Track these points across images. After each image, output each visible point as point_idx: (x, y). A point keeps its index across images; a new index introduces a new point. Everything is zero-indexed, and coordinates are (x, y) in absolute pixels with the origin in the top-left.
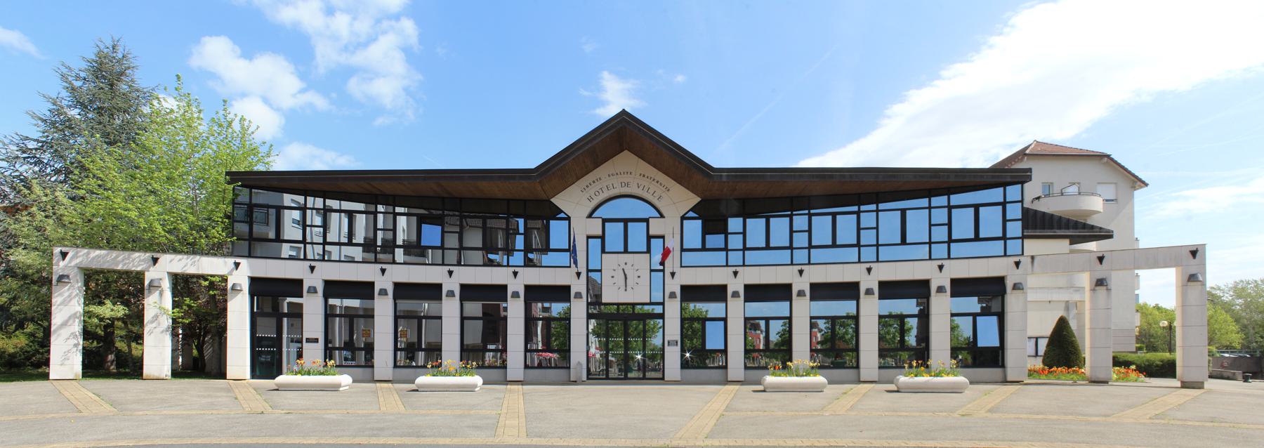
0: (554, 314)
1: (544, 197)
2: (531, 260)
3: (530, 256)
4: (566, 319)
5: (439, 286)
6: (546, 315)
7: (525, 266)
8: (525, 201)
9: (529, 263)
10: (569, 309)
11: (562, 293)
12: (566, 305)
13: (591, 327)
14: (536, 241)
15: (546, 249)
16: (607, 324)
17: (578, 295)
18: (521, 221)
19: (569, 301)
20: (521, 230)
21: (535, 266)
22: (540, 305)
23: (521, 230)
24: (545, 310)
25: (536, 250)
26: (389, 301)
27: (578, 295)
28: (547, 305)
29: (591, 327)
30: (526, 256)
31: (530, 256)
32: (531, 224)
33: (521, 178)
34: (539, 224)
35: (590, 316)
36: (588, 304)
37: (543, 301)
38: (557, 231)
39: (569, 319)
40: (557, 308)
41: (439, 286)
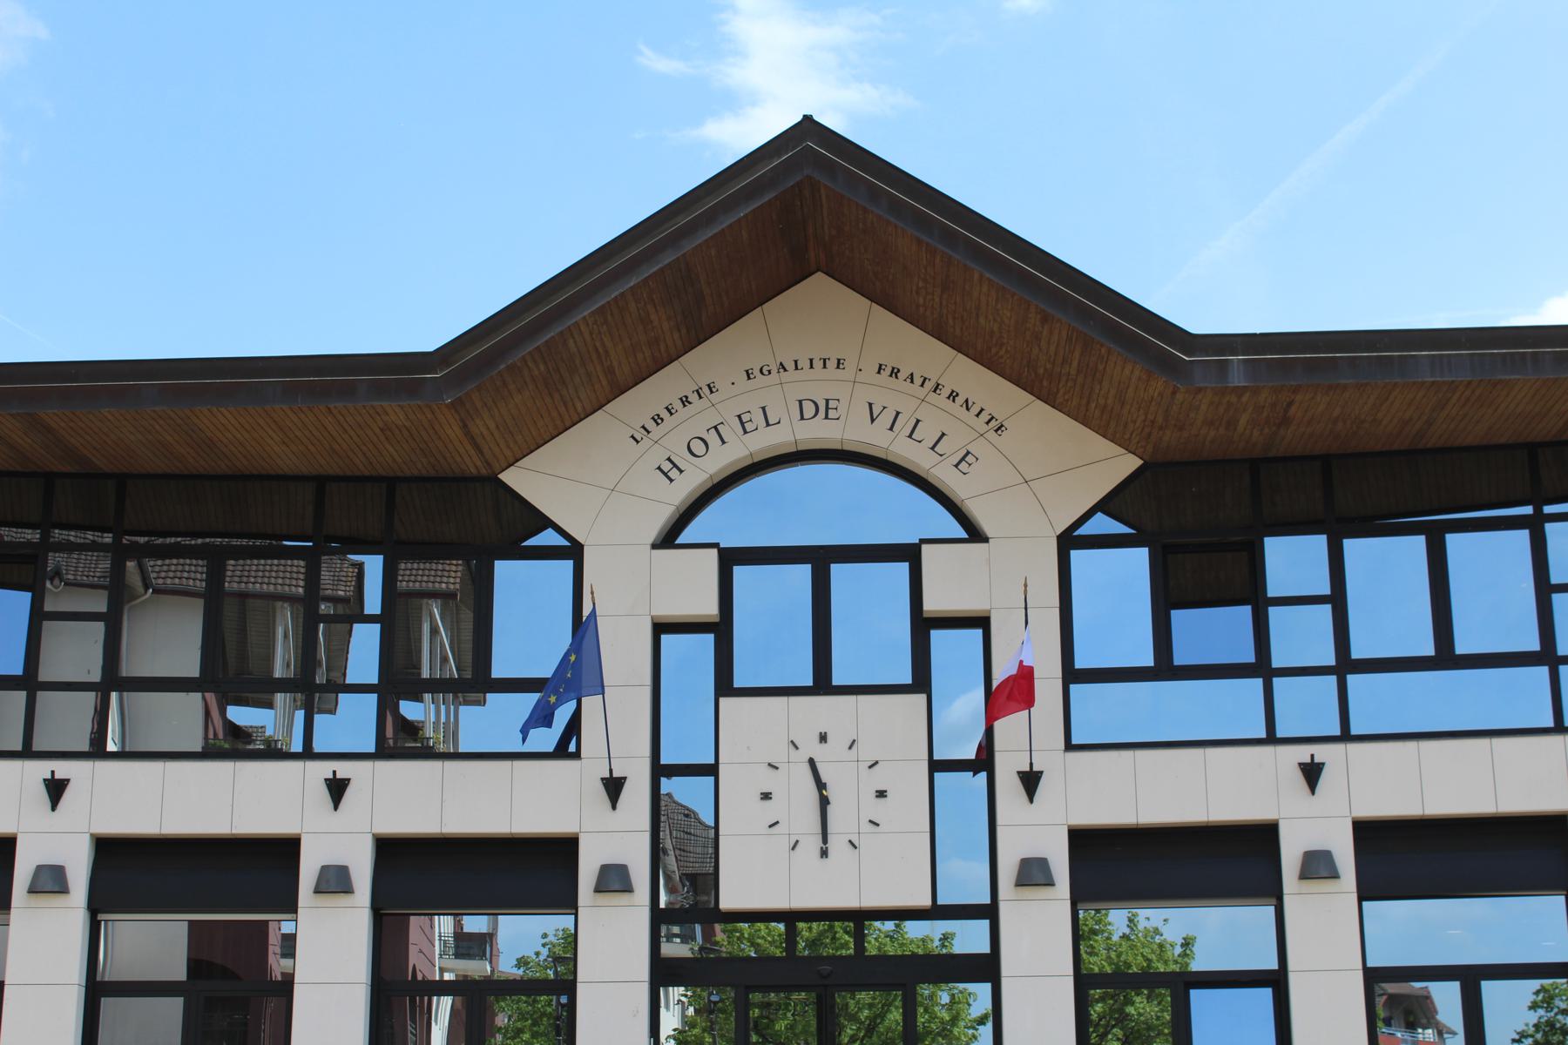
0: (507, 966)
1: (471, 464)
2: (410, 729)
3: (410, 710)
4: (556, 986)
5: (563, 850)
6: (477, 968)
7: (384, 752)
8: (391, 484)
9: (400, 743)
10: (572, 940)
11: (539, 869)
12: (554, 924)
13: (670, 1021)
14: (436, 647)
15: (477, 681)
16: (743, 1006)
17: (614, 879)
18: (374, 565)
19: (567, 901)
20: (373, 602)
21: (427, 753)
22: (444, 925)
23: (373, 602)
24: (470, 946)
25: (438, 686)
26: (68, 916)
27: (614, 879)
28: (475, 924)
29: (670, 1021)
30: (386, 708)
31: (410, 710)
32: (413, 575)
33: (380, 390)
34: (451, 575)
35: (663, 973)
36: (659, 918)
37: (458, 904)
38: (527, 613)
39: (567, 986)
40: (520, 937)
41: (563, 850)
